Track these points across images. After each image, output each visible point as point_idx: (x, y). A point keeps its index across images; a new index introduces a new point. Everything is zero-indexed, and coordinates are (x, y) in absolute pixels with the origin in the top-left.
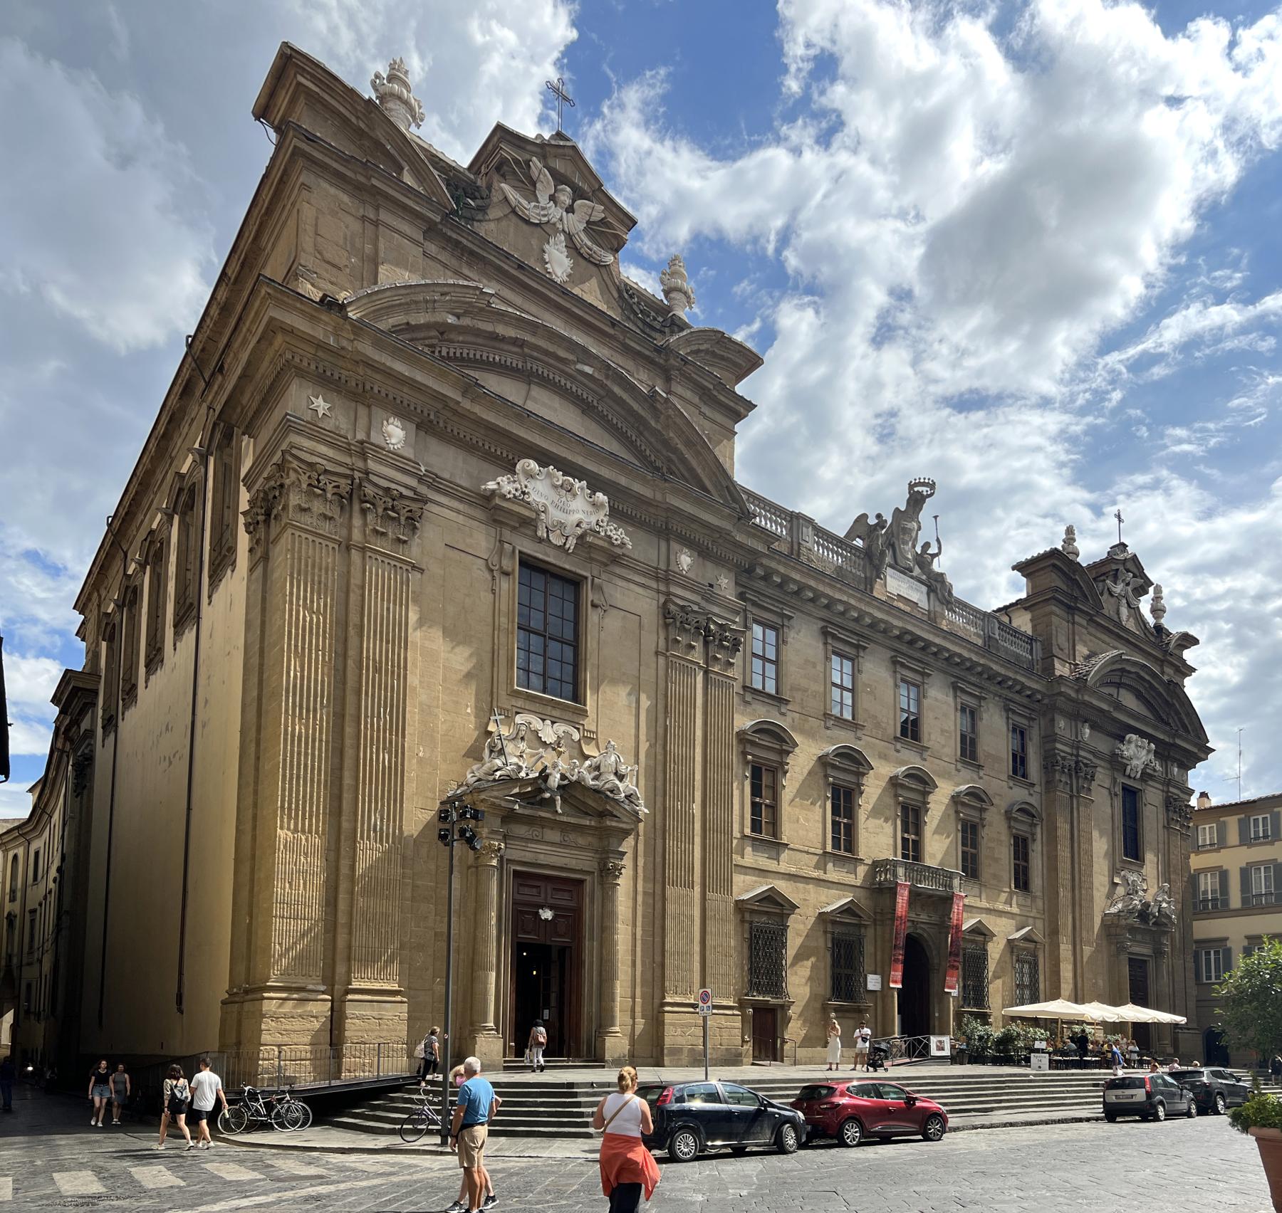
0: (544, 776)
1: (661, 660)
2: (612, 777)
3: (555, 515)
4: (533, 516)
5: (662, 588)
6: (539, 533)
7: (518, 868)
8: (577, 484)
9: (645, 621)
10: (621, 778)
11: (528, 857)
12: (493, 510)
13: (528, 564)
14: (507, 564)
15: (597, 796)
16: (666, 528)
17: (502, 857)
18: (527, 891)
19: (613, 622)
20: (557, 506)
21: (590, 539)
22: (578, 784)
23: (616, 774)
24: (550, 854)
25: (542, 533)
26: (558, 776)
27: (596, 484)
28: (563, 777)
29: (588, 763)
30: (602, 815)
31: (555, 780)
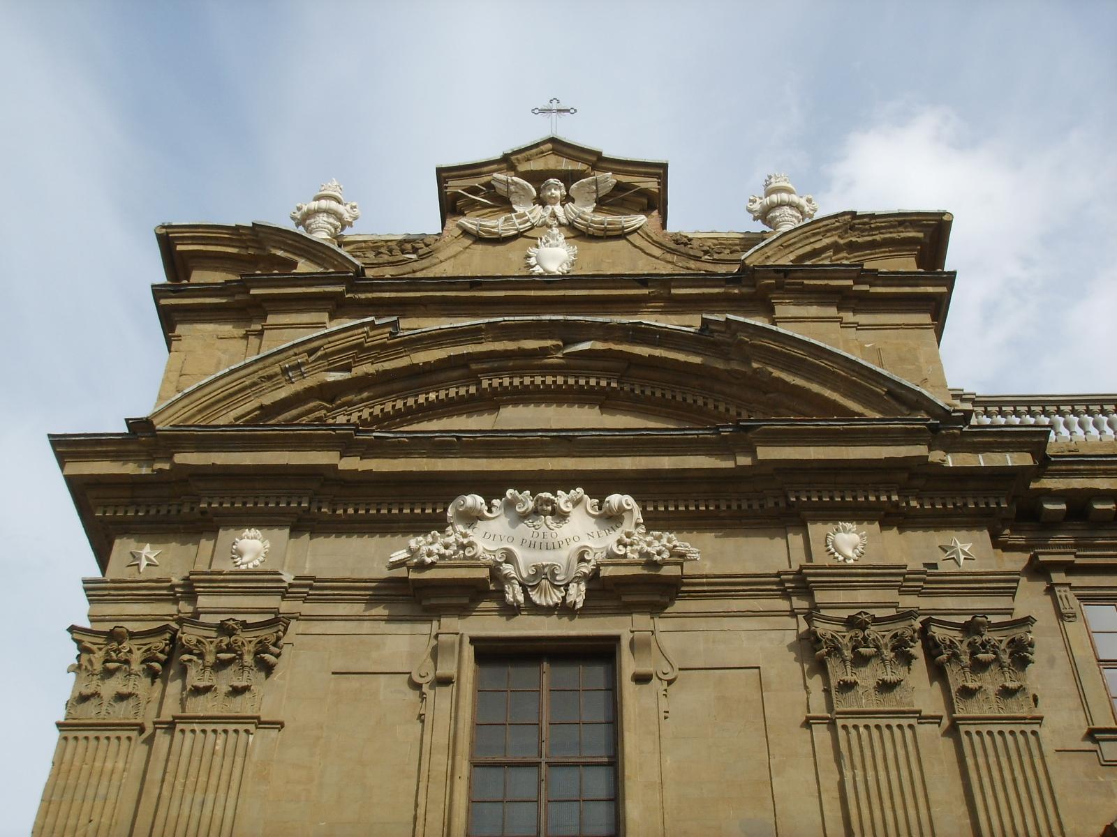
1: (821, 733)
3: (527, 560)
4: (484, 573)
5: (800, 604)
6: (509, 597)
8: (562, 499)
9: (770, 672)
12: (413, 596)
13: (491, 653)
14: (447, 668)
16: (778, 502)
19: (691, 698)
20: (532, 546)
21: (606, 572)
25: (514, 594)
27: (598, 485)
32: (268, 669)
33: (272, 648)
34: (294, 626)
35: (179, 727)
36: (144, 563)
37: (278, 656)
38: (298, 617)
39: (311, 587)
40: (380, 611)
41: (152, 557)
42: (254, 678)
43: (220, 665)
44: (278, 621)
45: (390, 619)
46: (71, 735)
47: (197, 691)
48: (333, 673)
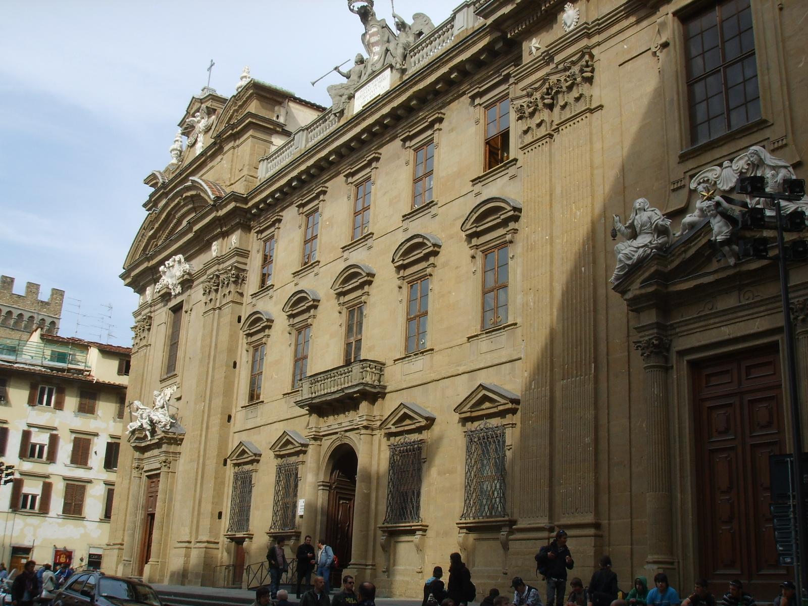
32: (590, 80)
33: (586, 69)
34: (595, 52)
35: (560, 129)
36: (534, 50)
37: (592, 71)
38: (599, 44)
39: (599, 25)
40: (632, 19)
41: (537, 45)
42: (585, 89)
43: (570, 88)
44: (587, 52)
45: (638, 22)
46: (526, 151)
47: (563, 107)
48: (619, 66)
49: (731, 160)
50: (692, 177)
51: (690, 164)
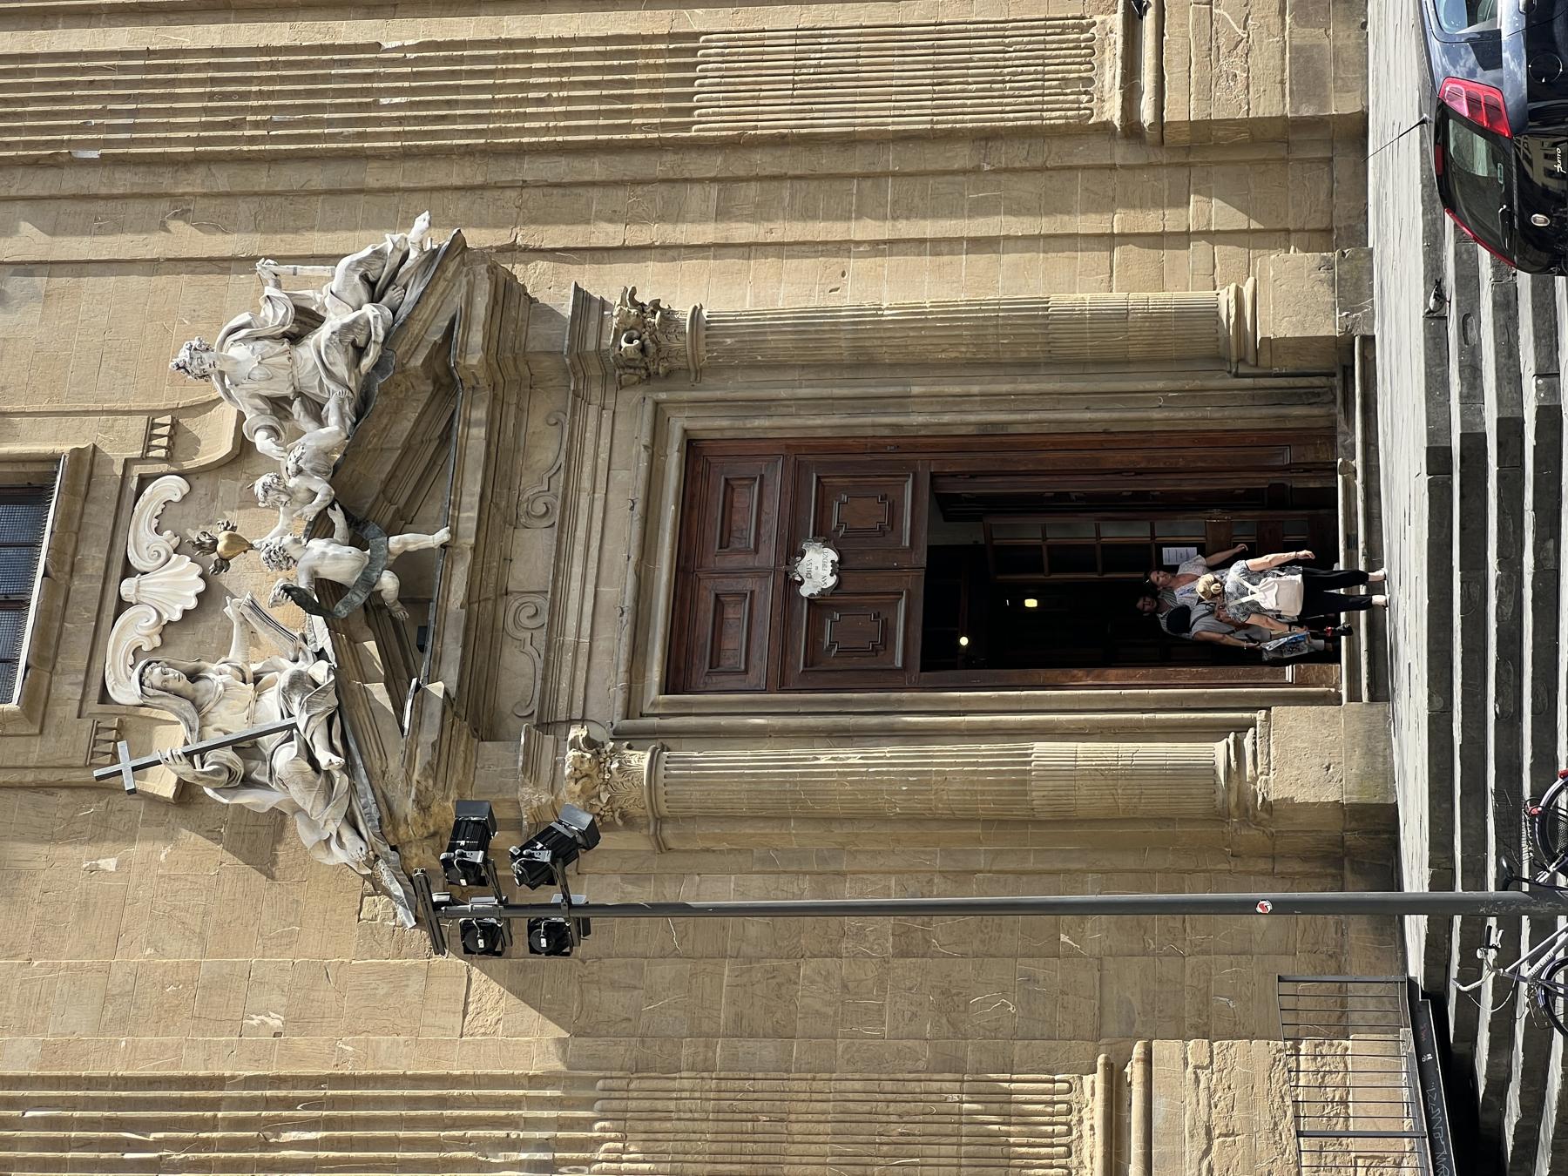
0: (321, 596)
2: (307, 352)
7: (655, 674)
10: (307, 319)
11: (613, 641)
15: (378, 402)
17: (618, 735)
18: (734, 642)
22: (340, 472)
23: (294, 338)
24: (591, 558)
26: (317, 545)
28: (320, 527)
29: (262, 442)
30: (446, 383)
31: (335, 558)
49: (128, 571)
50: (104, 697)
51: (68, 689)
